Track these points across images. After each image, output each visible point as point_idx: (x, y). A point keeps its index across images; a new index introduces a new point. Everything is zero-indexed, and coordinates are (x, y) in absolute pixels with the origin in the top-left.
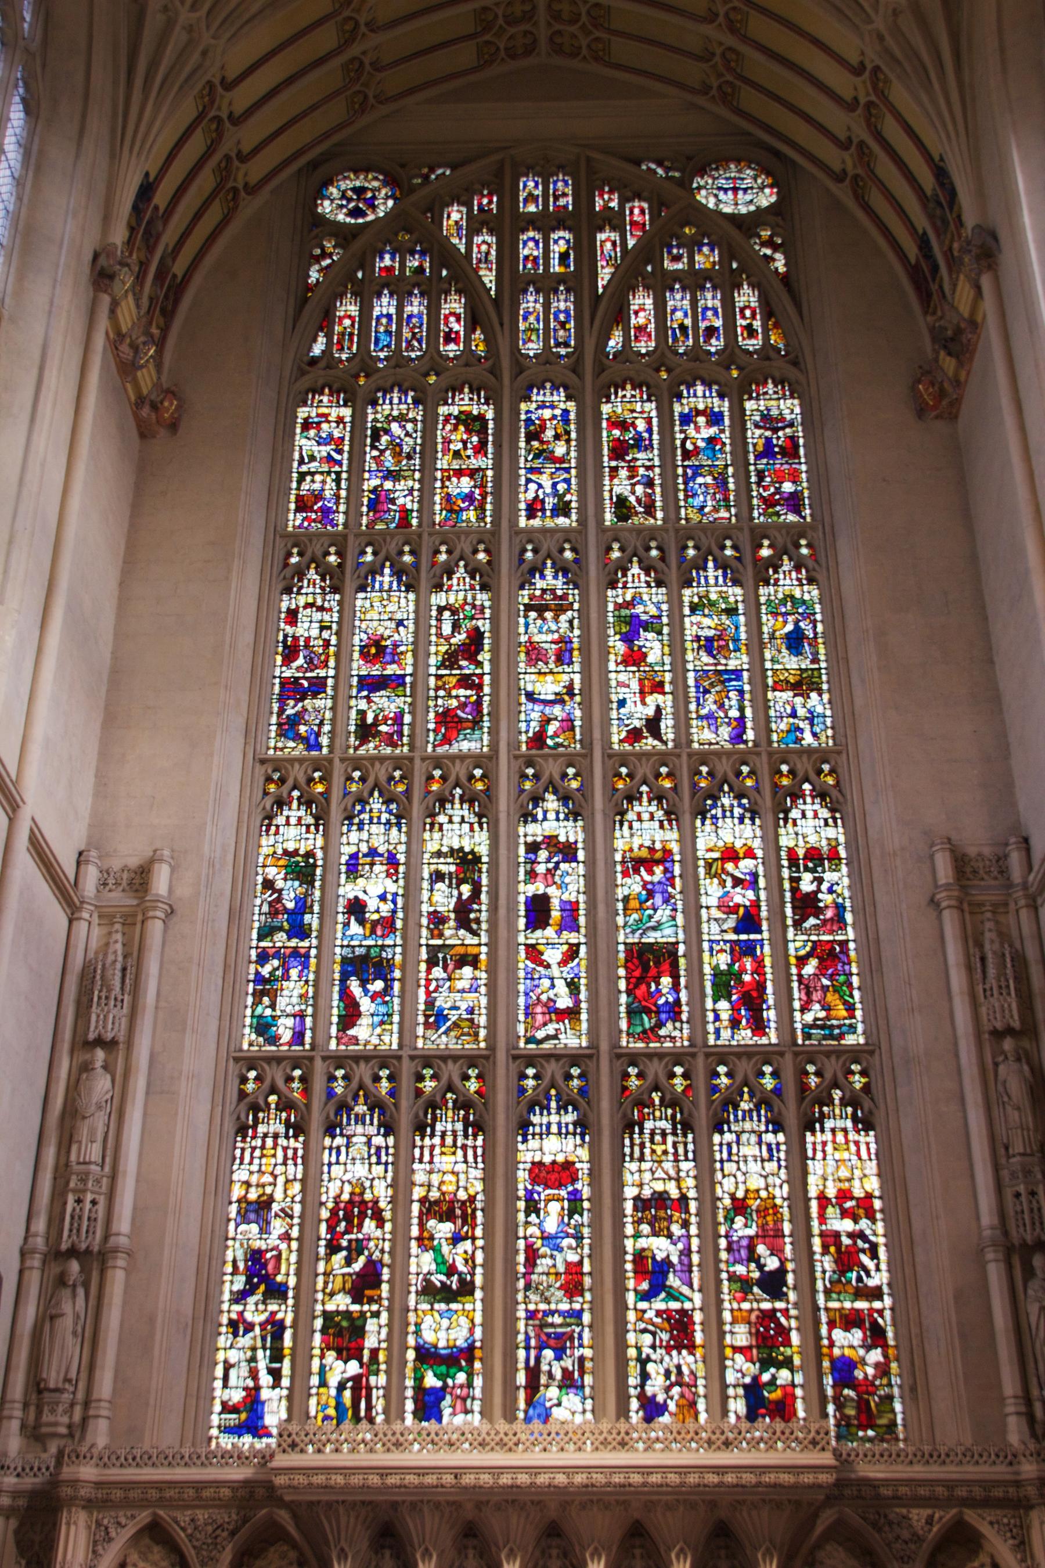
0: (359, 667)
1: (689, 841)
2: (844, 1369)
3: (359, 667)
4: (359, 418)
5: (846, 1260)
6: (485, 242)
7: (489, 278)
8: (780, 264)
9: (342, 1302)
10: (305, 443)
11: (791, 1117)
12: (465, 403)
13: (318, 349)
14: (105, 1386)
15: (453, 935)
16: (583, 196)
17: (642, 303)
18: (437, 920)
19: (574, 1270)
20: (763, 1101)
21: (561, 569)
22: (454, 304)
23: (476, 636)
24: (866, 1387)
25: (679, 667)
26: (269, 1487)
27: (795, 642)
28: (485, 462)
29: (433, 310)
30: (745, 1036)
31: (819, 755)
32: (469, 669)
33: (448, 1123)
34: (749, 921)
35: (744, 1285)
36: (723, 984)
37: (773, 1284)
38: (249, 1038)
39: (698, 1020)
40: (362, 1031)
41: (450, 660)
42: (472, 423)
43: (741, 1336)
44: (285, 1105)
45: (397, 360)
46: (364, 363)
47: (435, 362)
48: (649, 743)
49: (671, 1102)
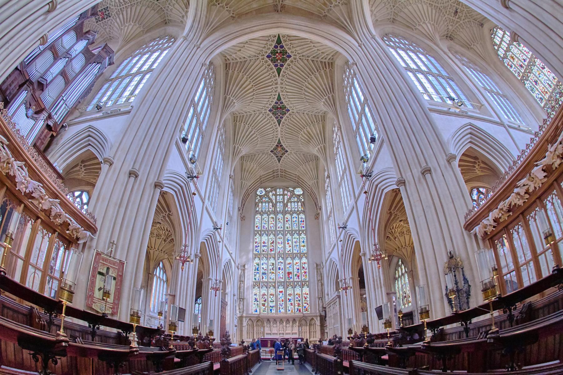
0: (263, 244)
1: (293, 262)
2: (305, 307)
3: (263, 244)
4: (262, 217)
5: (306, 298)
6: (274, 197)
7: (274, 201)
8: (303, 200)
9: (263, 302)
10: (256, 220)
11: (301, 287)
12: (272, 216)
13: (257, 209)
14: (245, 309)
15: (272, 271)
16: (283, 192)
17: (289, 204)
18: (270, 269)
19: (283, 300)
20: (299, 285)
21: (281, 234)
22: (271, 204)
23: (273, 241)
24: (307, 308)
25: (292, 245)
26: (259, 317)
27: (303, 242)
28: (274, 222)
29: (269, 205)
30: (298, 280)
31: (306, 253)
32: (272, 244)
33: (272, 288)
34: (298, 270)
35: (297, 301)
36: (296, 276)
37: (299, 301)
38: (254, 280)
39: (294, 278)
40: (264, 279)
41: (271, 244)
42: (273, 218)
43: (297, 305)
44: (257, 286)
45: (265, 211)
46: (262, 211)
47: (269, 211)
48: (290, 252)
49: (291, 286)
